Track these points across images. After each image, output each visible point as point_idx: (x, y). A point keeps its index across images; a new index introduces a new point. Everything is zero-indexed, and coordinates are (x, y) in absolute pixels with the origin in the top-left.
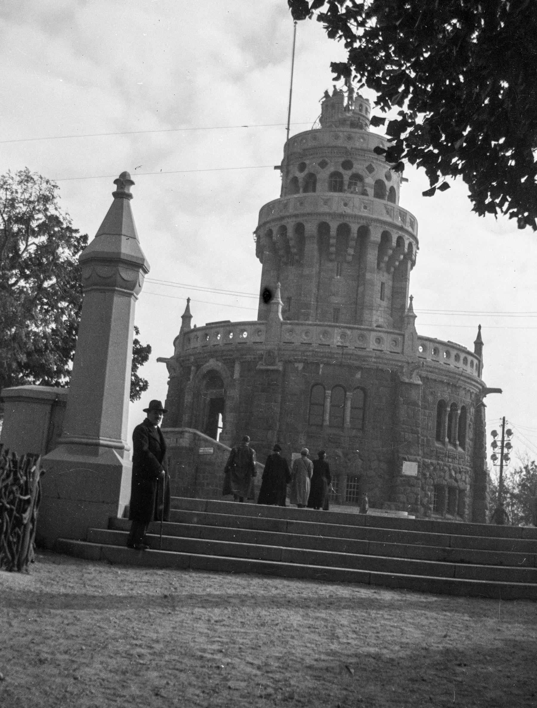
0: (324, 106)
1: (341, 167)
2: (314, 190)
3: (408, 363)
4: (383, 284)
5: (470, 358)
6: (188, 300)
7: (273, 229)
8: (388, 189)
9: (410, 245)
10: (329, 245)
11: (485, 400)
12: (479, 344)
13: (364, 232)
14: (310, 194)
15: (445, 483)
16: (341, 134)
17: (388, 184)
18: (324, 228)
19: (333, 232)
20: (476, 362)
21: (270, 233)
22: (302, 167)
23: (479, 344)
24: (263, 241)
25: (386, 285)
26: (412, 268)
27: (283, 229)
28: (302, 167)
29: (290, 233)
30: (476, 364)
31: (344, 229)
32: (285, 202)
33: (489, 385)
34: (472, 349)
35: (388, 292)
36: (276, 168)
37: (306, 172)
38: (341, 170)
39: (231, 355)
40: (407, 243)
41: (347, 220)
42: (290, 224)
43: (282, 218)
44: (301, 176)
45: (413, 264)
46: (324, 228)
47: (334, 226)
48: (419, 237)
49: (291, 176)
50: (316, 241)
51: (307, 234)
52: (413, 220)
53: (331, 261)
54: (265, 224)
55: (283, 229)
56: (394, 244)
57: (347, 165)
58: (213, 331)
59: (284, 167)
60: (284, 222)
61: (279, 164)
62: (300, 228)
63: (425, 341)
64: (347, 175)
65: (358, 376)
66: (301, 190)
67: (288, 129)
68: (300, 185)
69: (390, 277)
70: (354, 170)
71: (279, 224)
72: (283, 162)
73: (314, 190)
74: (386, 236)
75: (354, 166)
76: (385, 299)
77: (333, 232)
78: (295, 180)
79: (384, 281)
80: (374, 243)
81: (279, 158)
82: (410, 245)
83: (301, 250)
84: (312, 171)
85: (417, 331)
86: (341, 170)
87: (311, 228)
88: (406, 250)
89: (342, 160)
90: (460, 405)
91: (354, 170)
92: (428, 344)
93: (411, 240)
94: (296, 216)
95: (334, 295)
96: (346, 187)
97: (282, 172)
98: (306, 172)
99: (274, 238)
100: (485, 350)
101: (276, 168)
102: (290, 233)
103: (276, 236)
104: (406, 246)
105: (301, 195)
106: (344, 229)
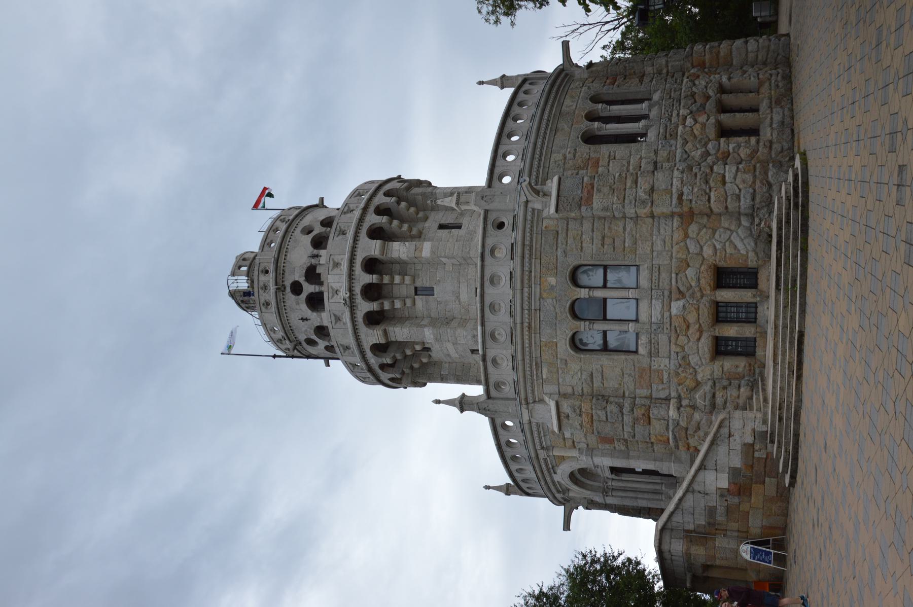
1: (300, 296)
3: (527, 202)
4: (442, 227)
5: (521, 96)
6: (487, 487)
9: (388, 194)
11: (582, 63)
12: (503, 82)
13: (371, 265)
15: (712, 120)
16: (262, 301)
17: (318, 229)
18: (373, 319)
19: (374, 306)
20: (526, 86)
22: (310, 342)
23: (503, 82)
25: (443, 222)
30: (530, 84)
31: (371, 292)
33: (560, 61)
34: (509, 92)
37: (314, 337)
38: (304, 296)
39: (545, 460)
41: (358, 289)
43: (370, 370)
48: (384, 178)
50: (390, 329)
52: (357, 192)
56: (384, 219)
57: (297, 288)
61: (322, 361)
63: (494, 174)
64: (308, 288)
67: (275, 356)
70: (302, 280)
74: (376, 233)
75: (297, 279)
80: (383, 251)
82: (388, 194)
83: (401, 345)
84: (312, 332)
86: (304, 296)
88: (394, 199)
89: (293, 297)
90: (590, 106)
91: (302, 280)
93: (381, 192)
95: (458, 297)
98: (314, 337)
100: (511, 72)
104: (388, 200)
106: (371, 292)
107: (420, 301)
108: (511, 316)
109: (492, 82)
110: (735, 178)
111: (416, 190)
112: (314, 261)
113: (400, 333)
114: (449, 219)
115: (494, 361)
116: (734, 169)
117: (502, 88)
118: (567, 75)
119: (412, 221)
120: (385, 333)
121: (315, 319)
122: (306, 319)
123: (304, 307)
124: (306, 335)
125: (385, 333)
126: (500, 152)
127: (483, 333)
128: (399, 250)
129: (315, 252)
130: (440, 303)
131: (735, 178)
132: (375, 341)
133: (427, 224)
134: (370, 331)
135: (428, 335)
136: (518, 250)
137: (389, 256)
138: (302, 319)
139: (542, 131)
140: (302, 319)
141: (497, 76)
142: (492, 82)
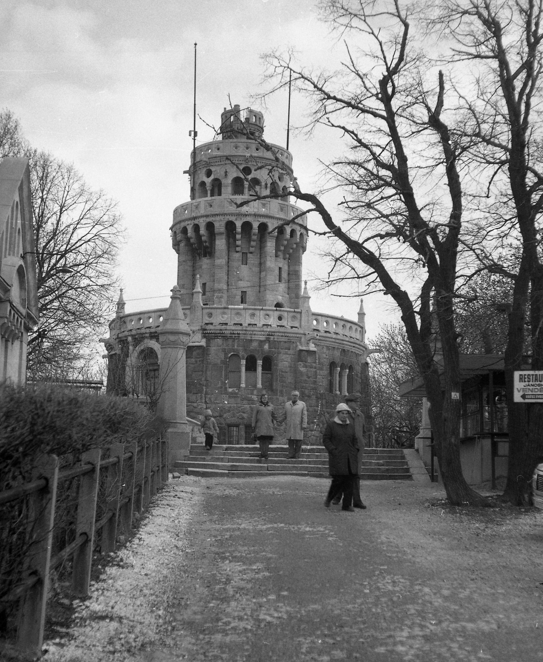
0: (224, 117)
2: (220, 194)
3: (305, 335)
4: (280, 268)
5: (354, 327)
7: (187, 227)
8: (281, 189)
10: (235, 240)
12: (361, 315)
14: (216, 197)
16: (239, 144)
18: (230, 226)
19: (239, 230)
20: (359, 329)
21: (185, 231)
22: (209, 173)
23: (361, 315)
24: (179, 237)
25: (283, 269)
26: (303, 254)
27: (196, 228)
28: (209, 173)
29: (203, 231)
32: (197, 204)
34: (355, 319)
35: (285, 275)
36: (185, 172)
37: (212, 177)
40: (298, 234)
41: (248, 219)
42: (202, 223)
43: (194, 218)
44: (208, 181)
45: (304, 249)
46: (230, 226)
47: (238, 224)
49: (199, 182)
50: (224, 236)
51: (216, 231)
53: (237, 252)
54: (180, 222)
55: (196, 228)
56: (288, 236)
58: (146, 315)
59: (193, 172)
60: (196, 222)
62: (210, 226)
65: (266, 347)
66: (209, 192)
68: (208, 188)
69: (286, 262)
71: (192, 222)
72: (190, 167)
73: (220, 194)
76: (283, 281)
77: (239, 230)
78: (203, 184)
79: (281, 266)
81: (187, 164)
85: (312, 309)
87: (220, 226)
88: (298, 240)
92: (319, 318)
93: (303, 231)
94: (207, 216)
95: (241, 280)
96: (246, 191)
97: (190, 175)
98: (212, 177)
99: (189, 235)
100: (366, 318)
101: (185, 172)
102: (203, 231)
103: (190, 232)
105: (209, 198)
106: (247, 226)
107: (238, 256)
108: (249, 324)
109: (361, 308)
110: (314, 436)
111: (301, 251)
112: (263, 184)
113: (221, 243)
114: (285, 275)
115: (224, 313)
116: (317, 435)
117: (358, 314)
118: (364, 351)
119: (284, 252)
120: (221, 234)
121: (228, 182)
122: (226, 175)
123: (235, 175)
124: (215, 171)
125: (221, 234)
126: (328, 319)
127: (240, 309)
128: (270, 245)
129: (269, 185)
130: (237, 268)
131: (314, 436)
132: (217, 225)
133: (282, 260)
134: (223, 224)
135: (221, 261)
136: (282, 330)
137: (268, 240)
138: (226, 172)
139: (337, 341)
140: (226, 172)
141: (365, 311)
142: (361, 308)
